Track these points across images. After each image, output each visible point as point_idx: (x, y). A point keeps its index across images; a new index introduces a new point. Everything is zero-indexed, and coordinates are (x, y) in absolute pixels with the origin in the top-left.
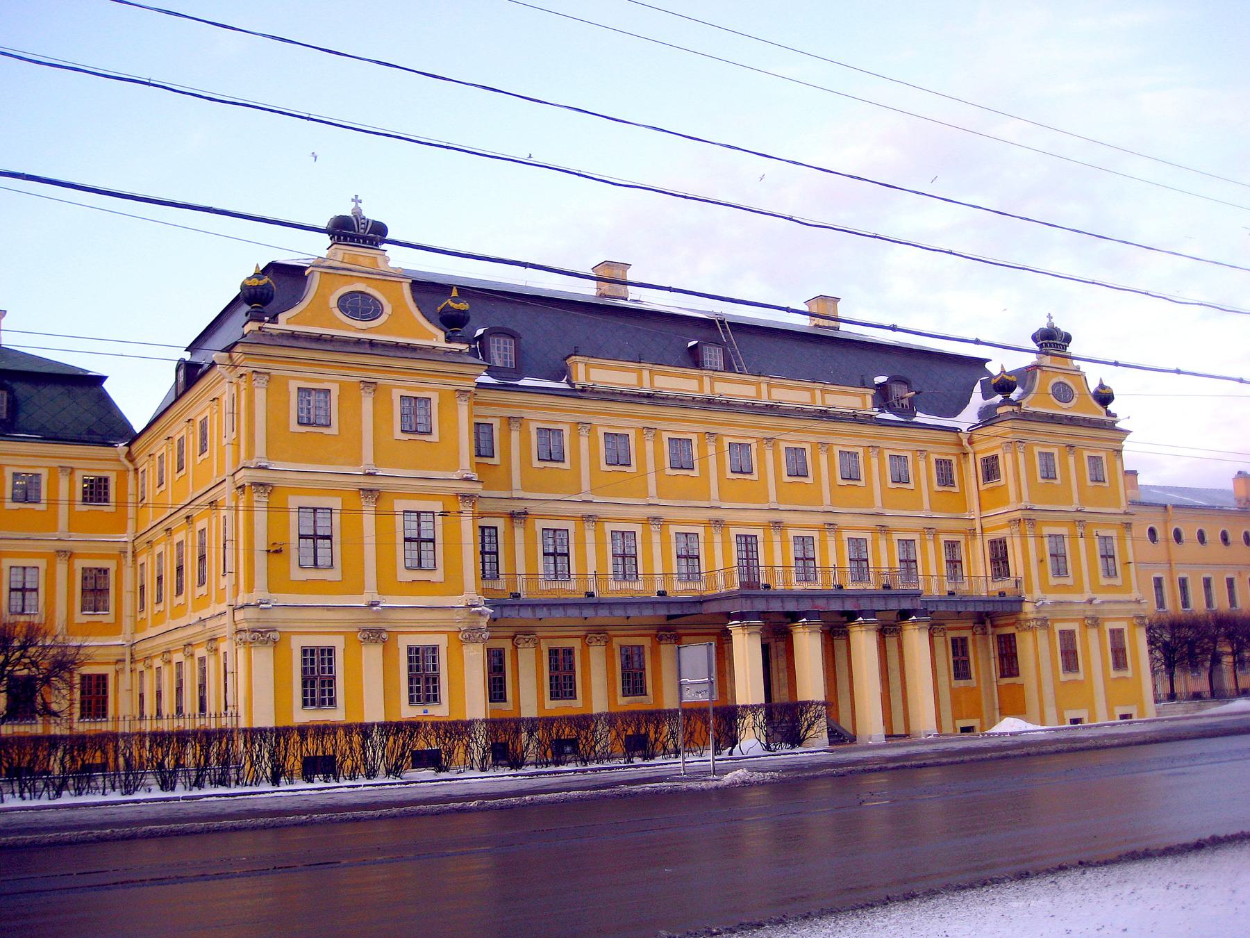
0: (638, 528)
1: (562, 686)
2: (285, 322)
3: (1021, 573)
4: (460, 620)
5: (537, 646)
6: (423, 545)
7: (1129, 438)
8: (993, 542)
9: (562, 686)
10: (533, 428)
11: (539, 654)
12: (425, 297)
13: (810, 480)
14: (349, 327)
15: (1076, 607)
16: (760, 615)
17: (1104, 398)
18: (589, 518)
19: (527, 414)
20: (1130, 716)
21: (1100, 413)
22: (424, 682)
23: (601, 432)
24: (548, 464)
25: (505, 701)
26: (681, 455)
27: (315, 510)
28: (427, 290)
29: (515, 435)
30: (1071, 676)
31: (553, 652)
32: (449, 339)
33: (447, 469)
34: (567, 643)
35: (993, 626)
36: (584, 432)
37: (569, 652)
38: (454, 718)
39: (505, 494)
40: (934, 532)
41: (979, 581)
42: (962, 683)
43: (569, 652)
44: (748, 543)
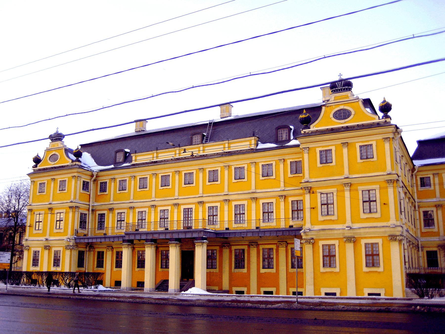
2: (313, 128)
4: (65, 243)
11: (231, 252)
13: (219, 182)
14: (50, 165)
15: (336, 232)
18: (131, 208)
20: (334, 294)
21: (374, 119)
22: (57, 262)
24: (121, 192)
26: (165, 181)
29: (113, 184)
38: (41, 271)
41: (281, 219)
42: (295, 270)
43: (103, 252)
44: (188, 212)
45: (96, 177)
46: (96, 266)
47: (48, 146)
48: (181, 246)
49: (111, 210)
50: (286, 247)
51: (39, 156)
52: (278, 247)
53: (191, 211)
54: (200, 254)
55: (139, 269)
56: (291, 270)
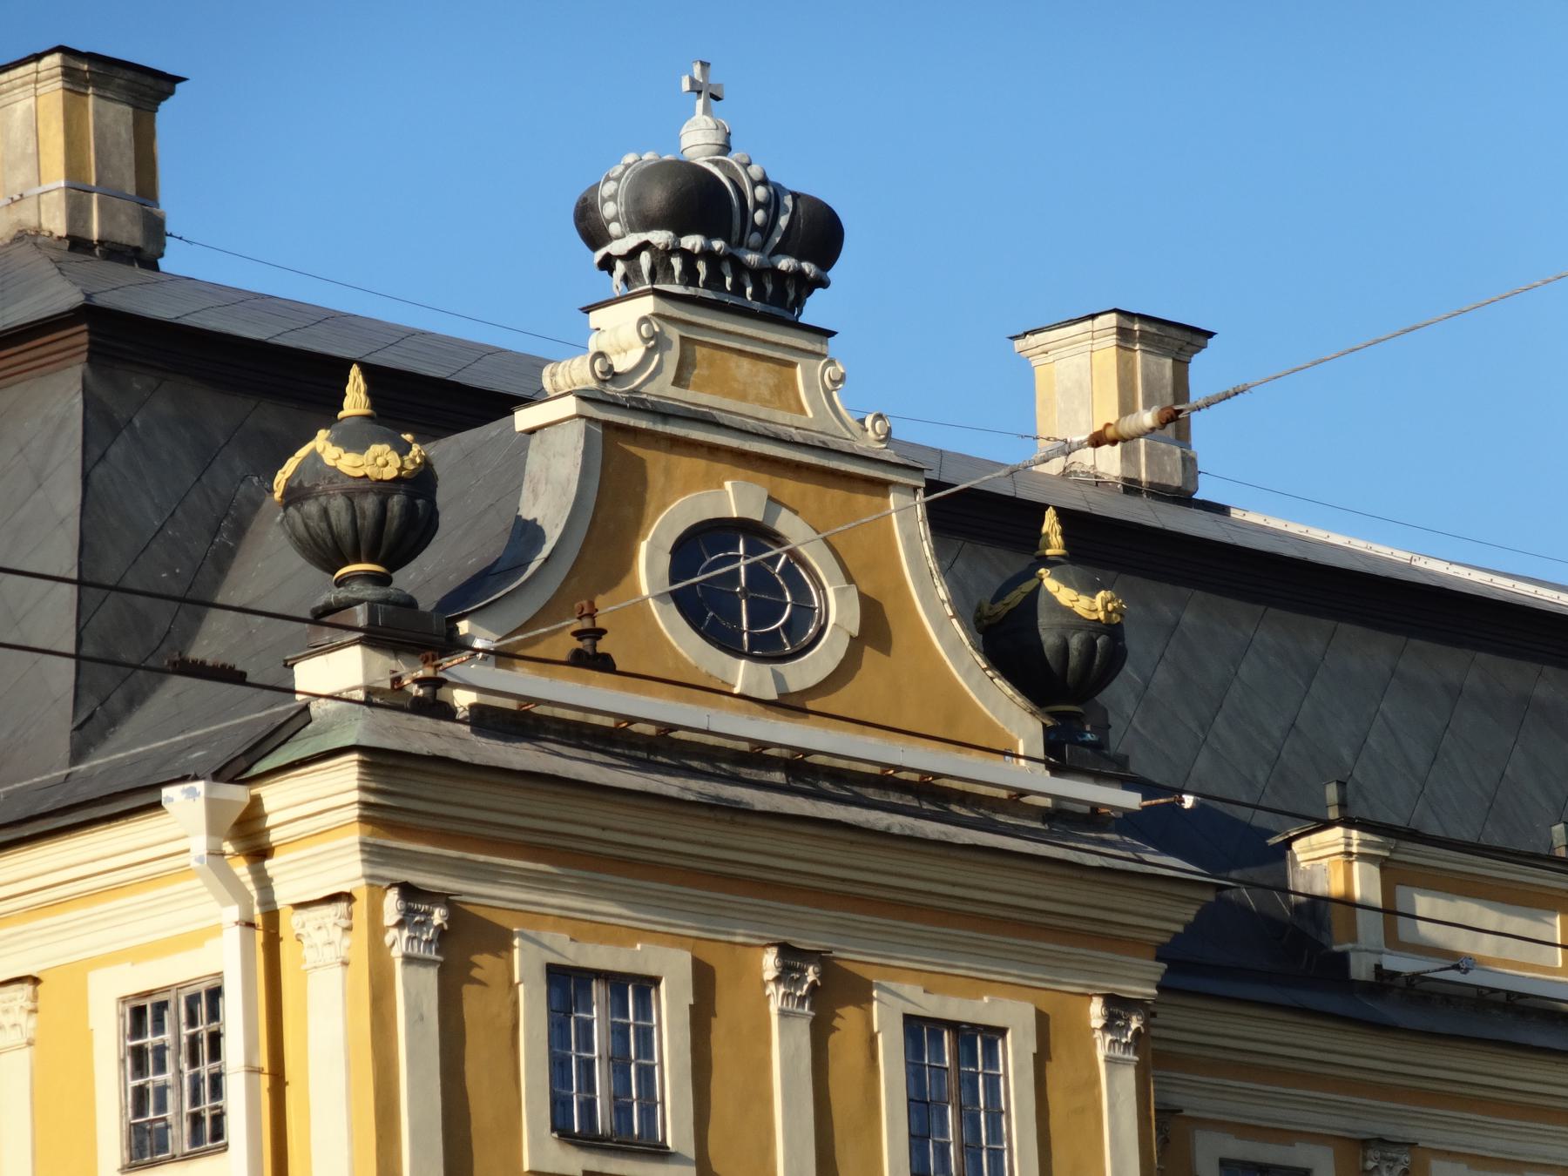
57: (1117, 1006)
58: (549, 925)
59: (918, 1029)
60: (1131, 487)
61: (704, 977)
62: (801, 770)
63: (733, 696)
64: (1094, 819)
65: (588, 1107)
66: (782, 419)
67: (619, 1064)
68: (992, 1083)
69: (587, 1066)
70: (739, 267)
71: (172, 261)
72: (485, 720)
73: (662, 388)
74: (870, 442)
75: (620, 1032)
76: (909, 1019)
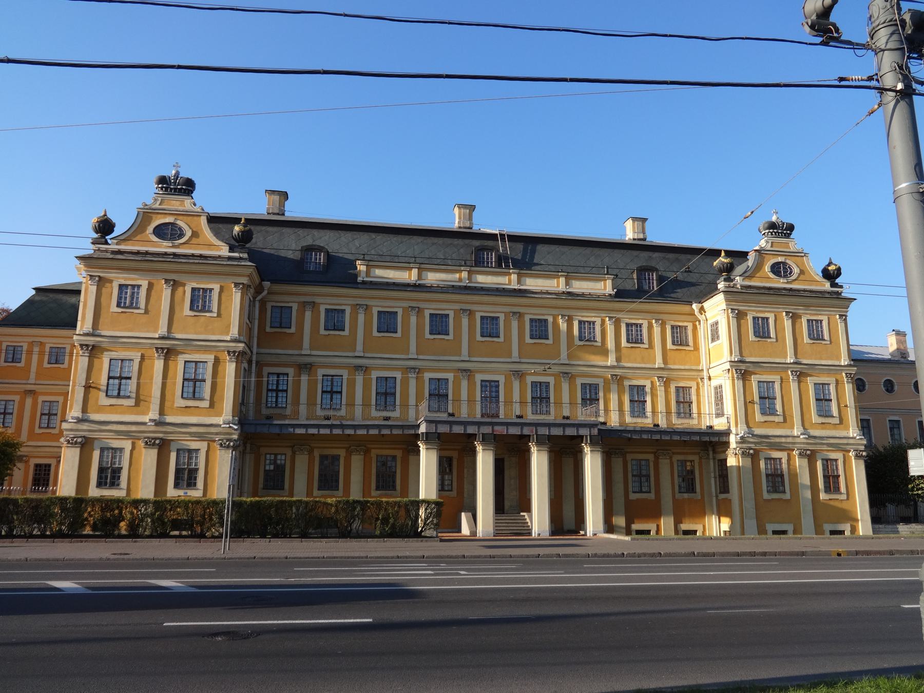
0: (398, 375)
1: (328, 480)
3: (730, 413)
5: (311, 452)
6: (329, 389)
7: (853, 305)
8: (716, 388)
9: (328, 480)
10: (322, 309)
12: (212, 225)
13: (550, 342)
16: (550, 438)
17: (831, 275)
18: (358, 368)
19: (318, 300)
23: (375, 311)
25: (283, 489)
26: (439, 324)
27: (122, 360)
28: (213, 220)
29: (308, 314)
30: (775, 496)
31: (323, 458)
32: (232, 249)
33: (221, 334)
34: (335, 452)
35: (714, 452)
36: (361, 311)
37: (336, 458)
39: (296, 352)
40: (520, 375)
42: (686, 496)
44: (490, 388)
45: (268, 293)
46: (261, 486)
47: (150, 201)
48: (440, 450)
49: (306, 367)
50: (671, 458)
51: (109, 216)
52: (657, 458)
53: (498, 386)
54: (592, 464)
55: (379, 492)
56: (678, 496)
57: (236, 285)
58: (119, 278)
59: (193, 289)
60: (460, 227)
61: (151, 286)
62: (175, 255)
63: (164, 246)
64: (241, 258)
65: (125, 303)
66: (181, 208)
67: (132, 298)
68: (210, 296)
69: (126, 298)
70: (171, 189)
71: (286, 214)
72: (113, 252)
73: (157, 206)
74: (199, 210)
75: (133, 293)
76: (120, 285)
